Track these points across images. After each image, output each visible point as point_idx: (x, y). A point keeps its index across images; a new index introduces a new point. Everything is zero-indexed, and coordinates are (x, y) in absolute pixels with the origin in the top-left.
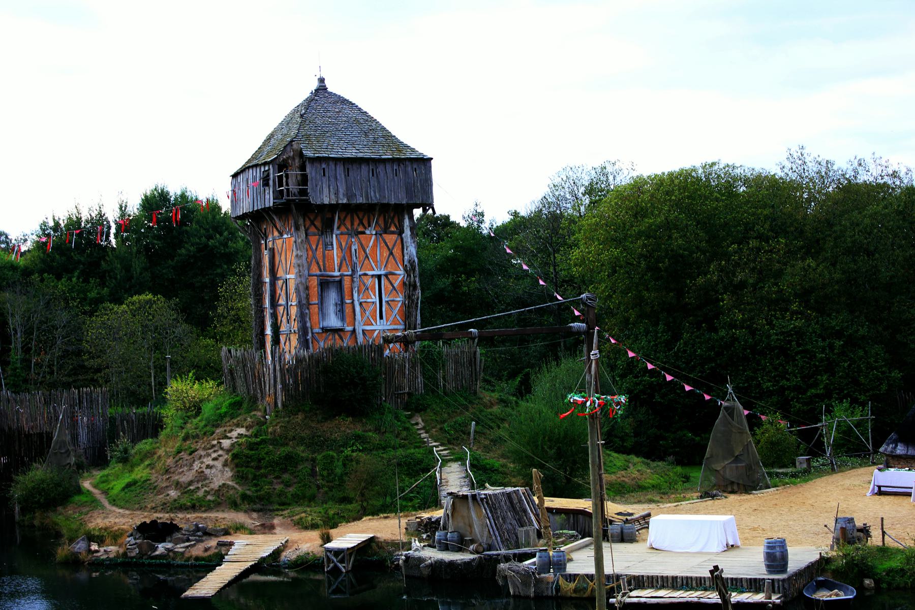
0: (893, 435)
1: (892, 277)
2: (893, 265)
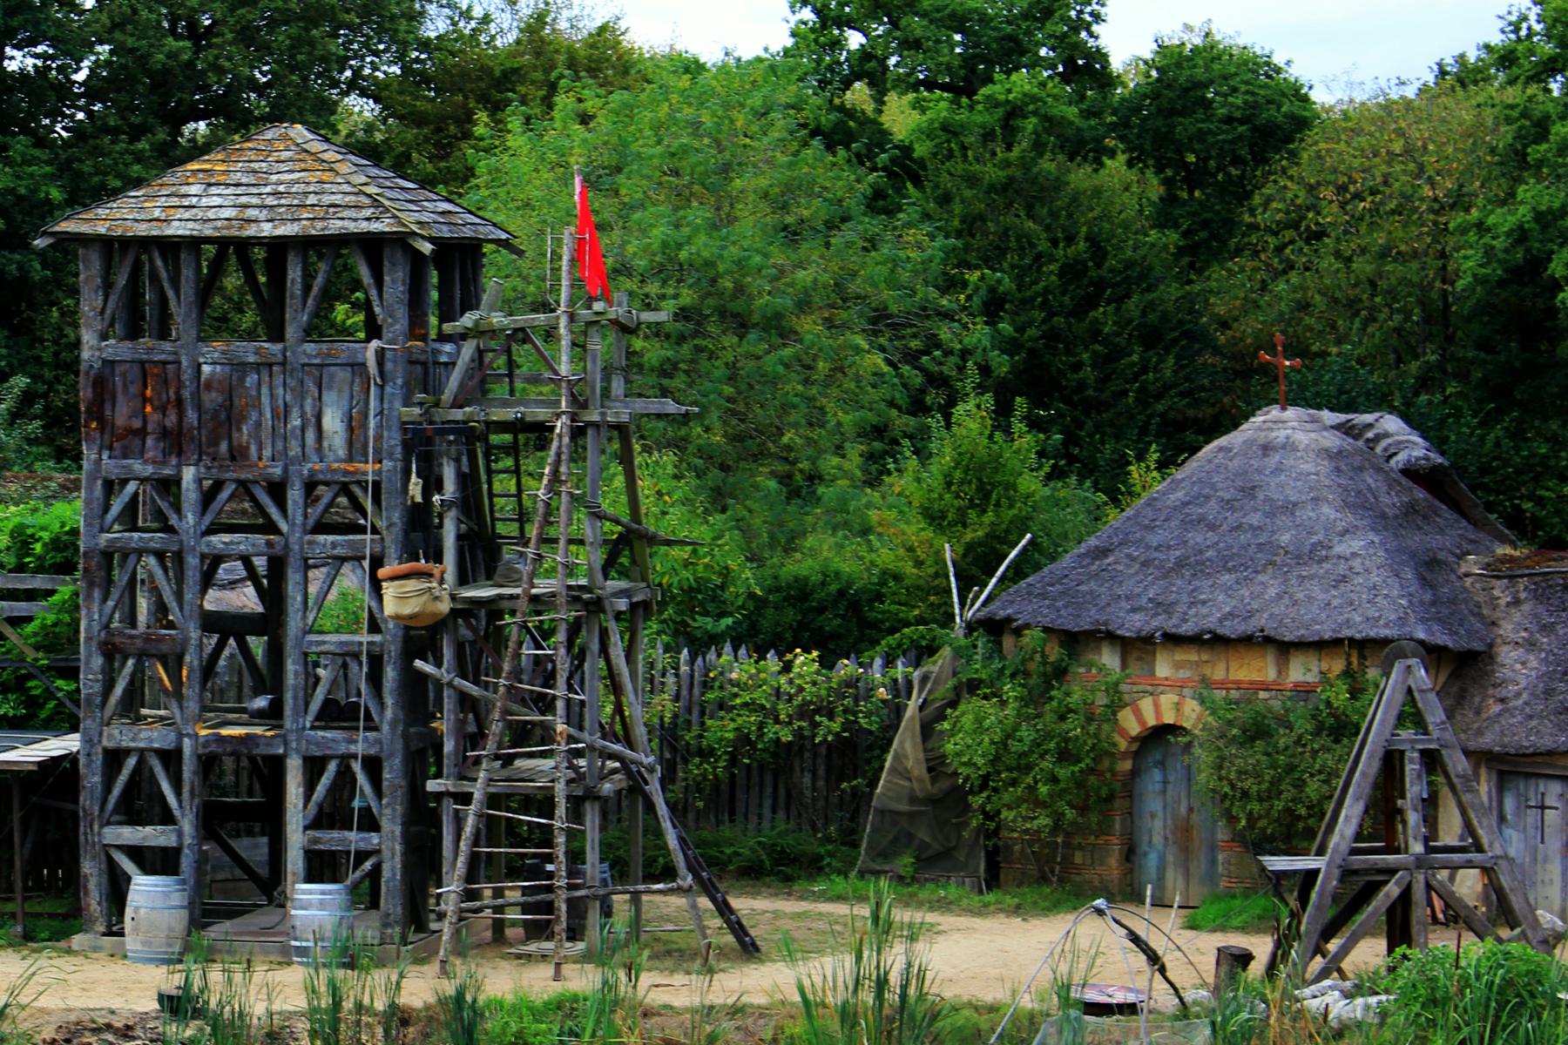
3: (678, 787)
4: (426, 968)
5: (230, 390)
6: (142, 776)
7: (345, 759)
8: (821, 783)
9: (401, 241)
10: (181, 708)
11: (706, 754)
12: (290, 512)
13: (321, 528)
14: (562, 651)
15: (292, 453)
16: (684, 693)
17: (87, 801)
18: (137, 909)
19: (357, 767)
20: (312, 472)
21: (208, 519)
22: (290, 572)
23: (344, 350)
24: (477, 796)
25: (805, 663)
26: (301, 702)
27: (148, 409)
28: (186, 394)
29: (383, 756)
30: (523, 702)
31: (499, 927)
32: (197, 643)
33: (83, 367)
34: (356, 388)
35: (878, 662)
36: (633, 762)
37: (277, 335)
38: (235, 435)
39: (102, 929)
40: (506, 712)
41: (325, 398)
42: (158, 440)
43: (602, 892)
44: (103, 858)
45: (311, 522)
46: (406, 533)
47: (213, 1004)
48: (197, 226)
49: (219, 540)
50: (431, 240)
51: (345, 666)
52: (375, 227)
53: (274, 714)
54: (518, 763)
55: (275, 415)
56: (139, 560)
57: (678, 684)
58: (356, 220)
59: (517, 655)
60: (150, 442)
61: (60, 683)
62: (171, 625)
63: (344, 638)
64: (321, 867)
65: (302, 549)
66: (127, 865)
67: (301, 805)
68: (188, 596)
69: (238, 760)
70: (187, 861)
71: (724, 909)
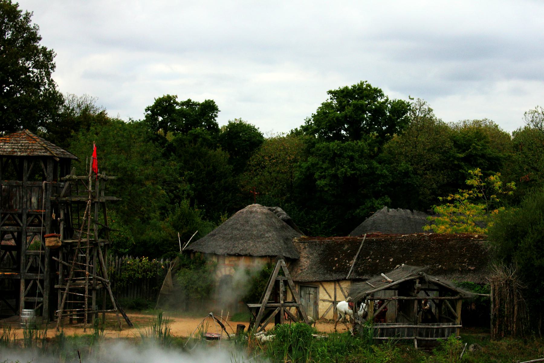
3: (115, 288)
8: (148, 288)
9: (52, 158)
11: (122, 280)
13: (30, 225)
14: (88, 255)
16: (117, 266)
19: (38, 282)
20: (29, 212)
21: (3, 223)
22: (23, 235)
23: (38, 183)
24: (67, 289)
25: (145, 259)
30: (78, 267)
31: (71, 320)
34: (40, 192)
35: (162, 260)
36: (104, 281)
37: (21, 179)
38: (10, 203)
40: (74, 269)
43: (96, 312)
45: (28, 224)
48: (2, 153)
49: (6, 228)
50: (59, 158)
51: (36, 258)
52: (45, 154)
53: (18, 270)
54: (77, 282)
57: (115, 264)
58: (41, 152)
59: (77, 257)
63: (35, 251)
64: (28, 306)
71: (125, 316)
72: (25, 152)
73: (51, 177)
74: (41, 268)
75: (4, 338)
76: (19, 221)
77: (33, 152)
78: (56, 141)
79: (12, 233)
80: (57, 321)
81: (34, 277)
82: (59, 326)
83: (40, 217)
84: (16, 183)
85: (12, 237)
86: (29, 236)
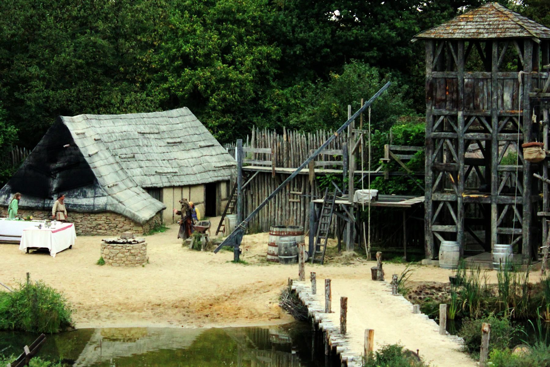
0: (7, 187)
1: (13, 36)
2: (15, 24)
4: (537, 272)
5: (474, 86)
6: (445, 210)
7: (511, 205)
9: (530, 39)
10: (457, 188)
12: (493, 126)
13: (503, 131)
15: (494, 107)
17: (427, 217)
18: (443, 251)
19: (514, 207)
20: (500, 113)
21: (466, 129)
23: (512, 74)
26: (496, 187)
27: (447, 93)
28: (460, 88)
29: (523, 204)
32: (462, 169)
33: (427, 80)
34: (515, 86)
37: (489, 69)
38: (475, 101)
39: (432, 258)
41: (504, 89)
42: (450, 103)
44: (432, 235)
45: (500, 129)
46: (531, 134)
47: (467, 282)
48: (463, 35)
49: (470, 135)
50: (540, 39)
51: (510, 176)
52: (521, 35)
53: (487, 190)
55: (488, 94)
56: (444, 141)
58: (515, 32)
60: (448, 103)
61: (418, 180)
62: (454, 162)
64: (503, 239)
65: (497, 138)
66: (440, 238)
67: (496, 219)
68: (460, 152)
69: (475, 205)
70: (459, 237)
72: (494, 33)
73: (531, 65)
74: (518, 190)
75: (472, 282)
76: (488, 126)
77: (504, 32)
78: (534, 17)
79: (478, 142)
80: (541, 261)
81: (510, 202)
82: (544, 267)
83: (515, 119)
84: (483, 75)
85: (478, 147)
86: (501, 145)
